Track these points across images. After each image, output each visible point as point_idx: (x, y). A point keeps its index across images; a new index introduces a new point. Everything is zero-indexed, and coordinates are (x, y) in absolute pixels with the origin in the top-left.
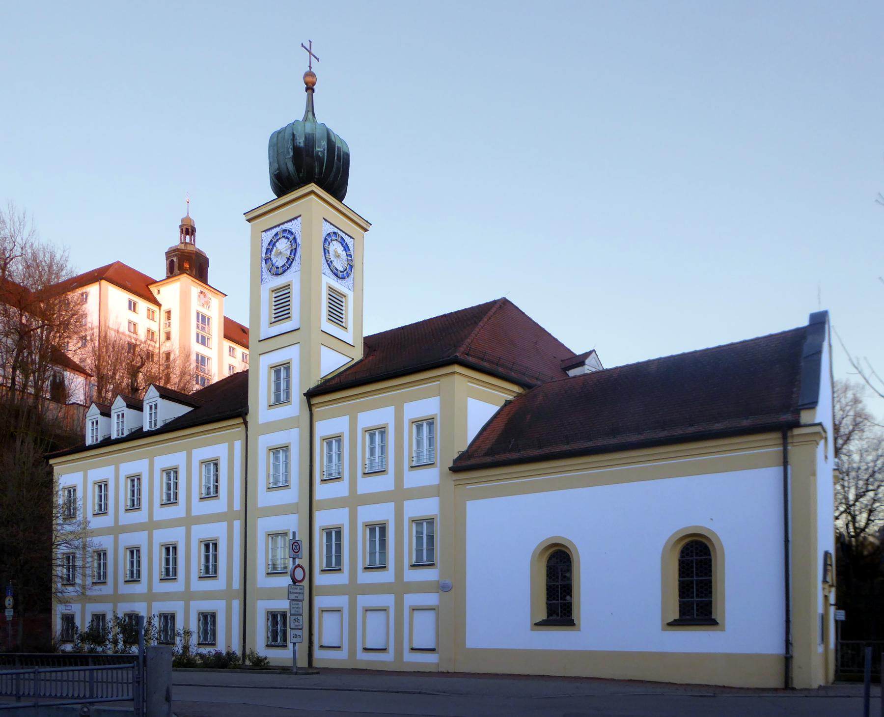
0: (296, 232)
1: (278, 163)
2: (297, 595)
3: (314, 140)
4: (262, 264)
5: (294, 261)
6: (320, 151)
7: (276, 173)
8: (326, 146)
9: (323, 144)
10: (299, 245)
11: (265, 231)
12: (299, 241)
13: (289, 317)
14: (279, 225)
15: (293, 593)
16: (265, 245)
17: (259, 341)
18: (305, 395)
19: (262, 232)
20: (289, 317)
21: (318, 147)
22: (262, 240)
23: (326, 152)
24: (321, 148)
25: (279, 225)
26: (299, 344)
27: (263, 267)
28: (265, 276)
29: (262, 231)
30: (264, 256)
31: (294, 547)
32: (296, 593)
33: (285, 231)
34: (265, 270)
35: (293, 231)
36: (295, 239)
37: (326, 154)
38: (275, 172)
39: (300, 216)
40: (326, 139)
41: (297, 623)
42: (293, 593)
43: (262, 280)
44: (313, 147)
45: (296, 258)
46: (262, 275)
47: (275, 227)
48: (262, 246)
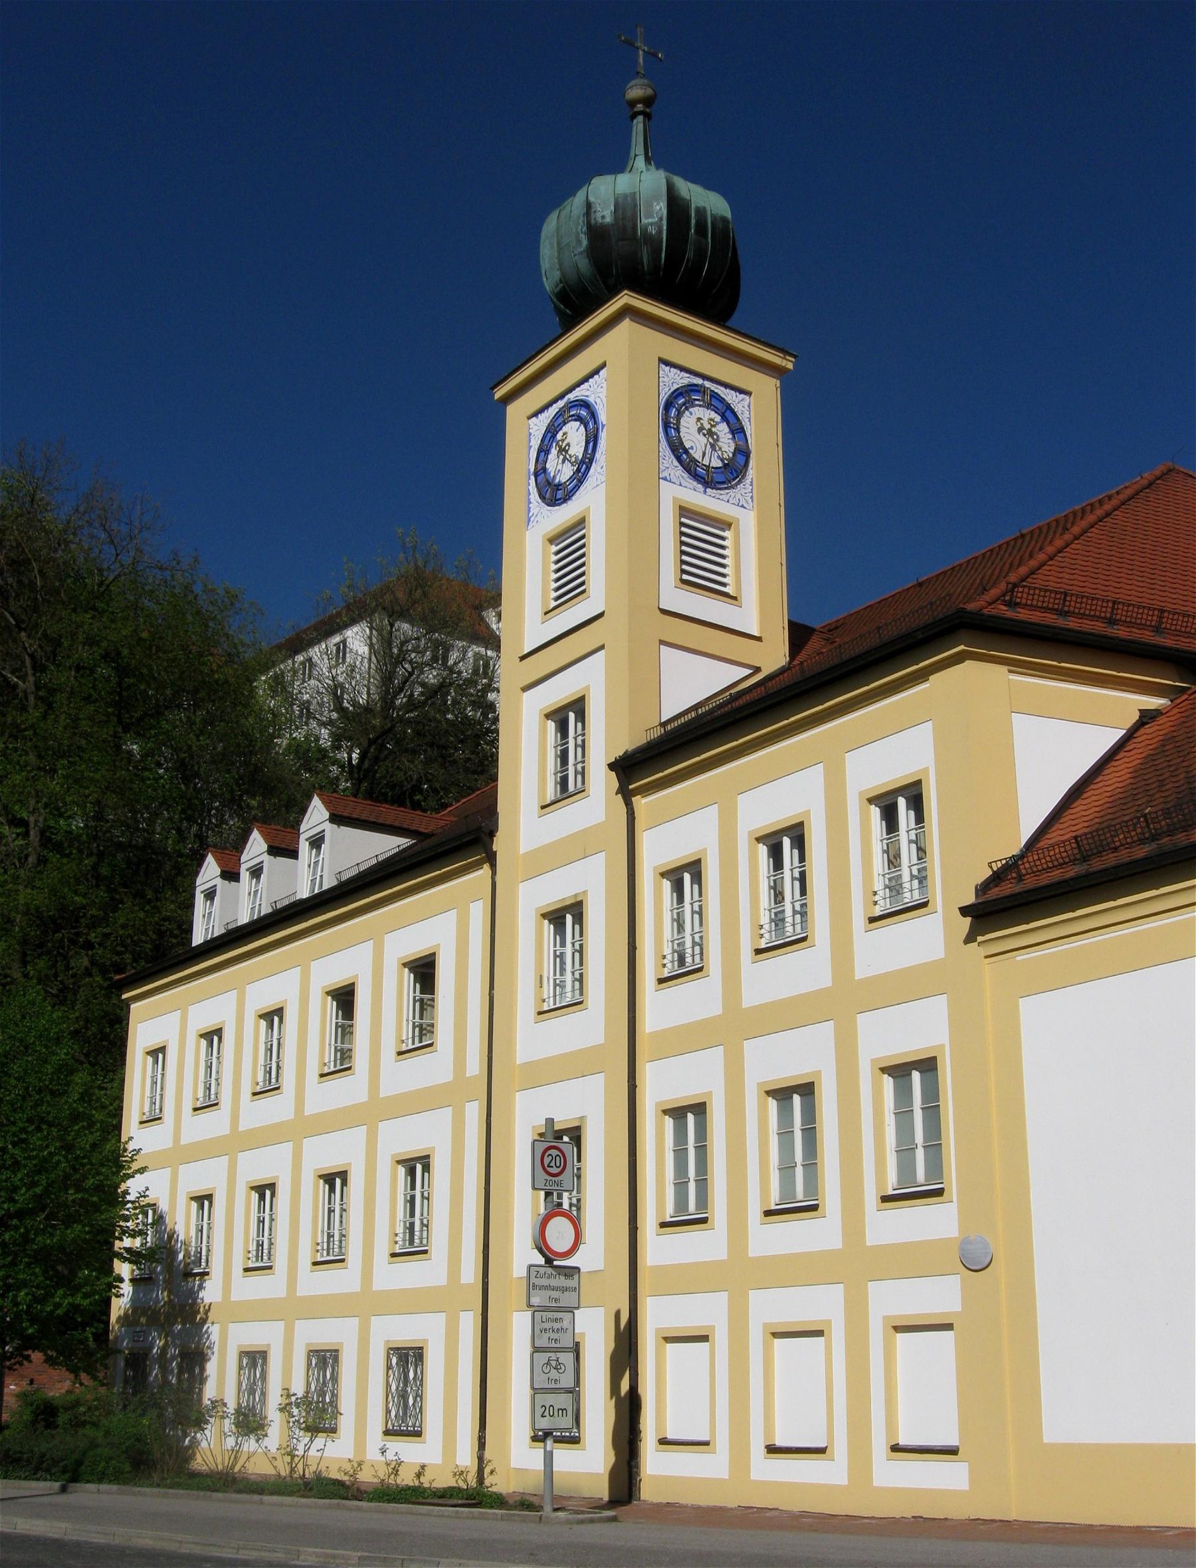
0: (598, 401)
1: (561, 268)
2: (555, 1294)
3: (636, 205)
4: (529, 485)
5: (594, 463)
6: (651, 224)
7: (558, 288)
8: (665, 212)
9: (658, 208)
10: (603, 426)
12: (602, 417)
13: (584, 592)
15: (542, 1288)
16: (535, 443)
17: (523, 658)
18: (612, 766)
19: (529, 418)
20: (584, 592)
21: (647, 217)
23: (665, 222)
24: (652, 217)
26: (603, 652)
28: (534, 510)
29: (529, 413)
31: (547, 1160)
32: (554, 1289)
34: (535, 496)
35: (591, 400)
36: (593, 415)
37: (665, 228)
39: (603, 366)
40: (665, 198)
41: (554, 1374)
42: (542, 1288)
43: (529, 520)
44: (634, 218)
45: (598, 455)
48: (531, 447)
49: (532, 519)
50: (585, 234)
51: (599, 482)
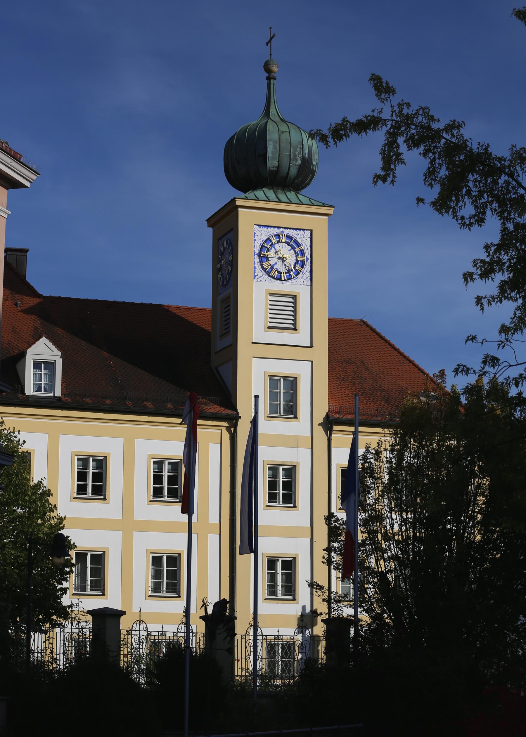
0: (303, 243)
5: (301, 273)
7: (273, 169)
11: (259, 226)
14: (279, 228)
17: (253, 343)
19: (255, 225)
22: (255, 234)
25: (279, 228)
27: (256, 262)
30: (257, 251)
33: (288, 237)
35: (299, 241)
38: (272, 168)
43: (255, 276)
46: (255, 272)
47: (274, 227)
48: (255, 240)
49: (257, 277)
50: (300, 157)
51: (305, 283)
